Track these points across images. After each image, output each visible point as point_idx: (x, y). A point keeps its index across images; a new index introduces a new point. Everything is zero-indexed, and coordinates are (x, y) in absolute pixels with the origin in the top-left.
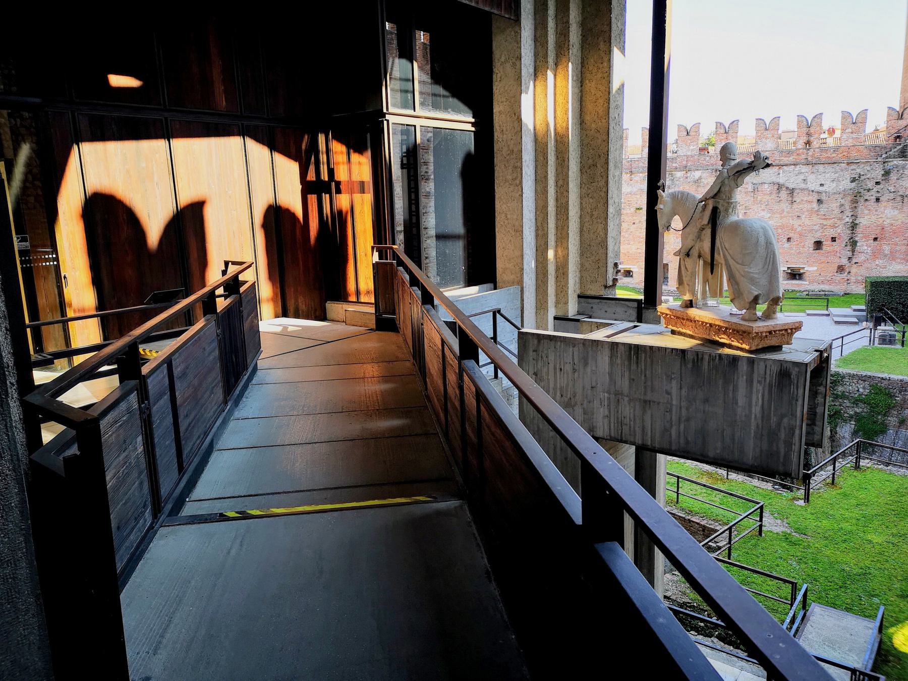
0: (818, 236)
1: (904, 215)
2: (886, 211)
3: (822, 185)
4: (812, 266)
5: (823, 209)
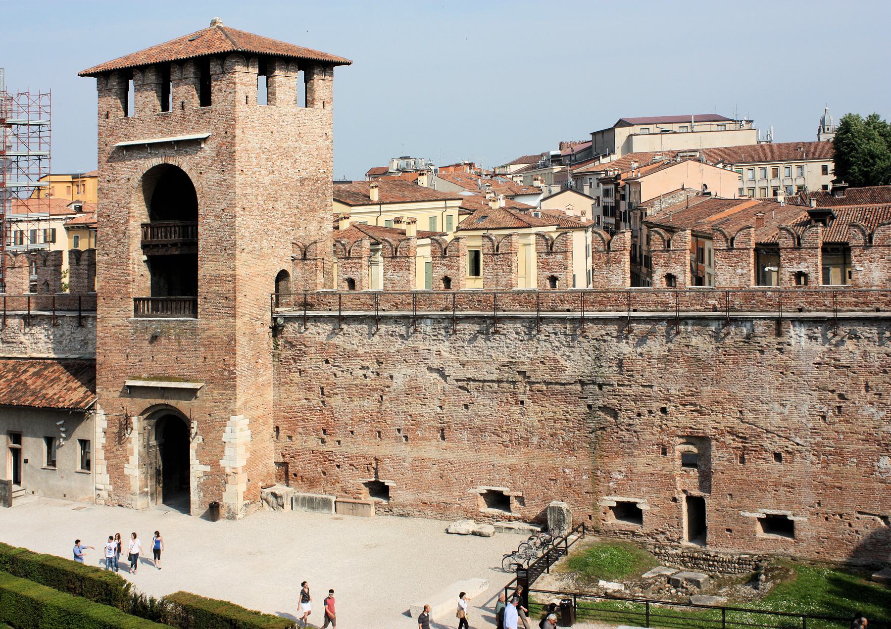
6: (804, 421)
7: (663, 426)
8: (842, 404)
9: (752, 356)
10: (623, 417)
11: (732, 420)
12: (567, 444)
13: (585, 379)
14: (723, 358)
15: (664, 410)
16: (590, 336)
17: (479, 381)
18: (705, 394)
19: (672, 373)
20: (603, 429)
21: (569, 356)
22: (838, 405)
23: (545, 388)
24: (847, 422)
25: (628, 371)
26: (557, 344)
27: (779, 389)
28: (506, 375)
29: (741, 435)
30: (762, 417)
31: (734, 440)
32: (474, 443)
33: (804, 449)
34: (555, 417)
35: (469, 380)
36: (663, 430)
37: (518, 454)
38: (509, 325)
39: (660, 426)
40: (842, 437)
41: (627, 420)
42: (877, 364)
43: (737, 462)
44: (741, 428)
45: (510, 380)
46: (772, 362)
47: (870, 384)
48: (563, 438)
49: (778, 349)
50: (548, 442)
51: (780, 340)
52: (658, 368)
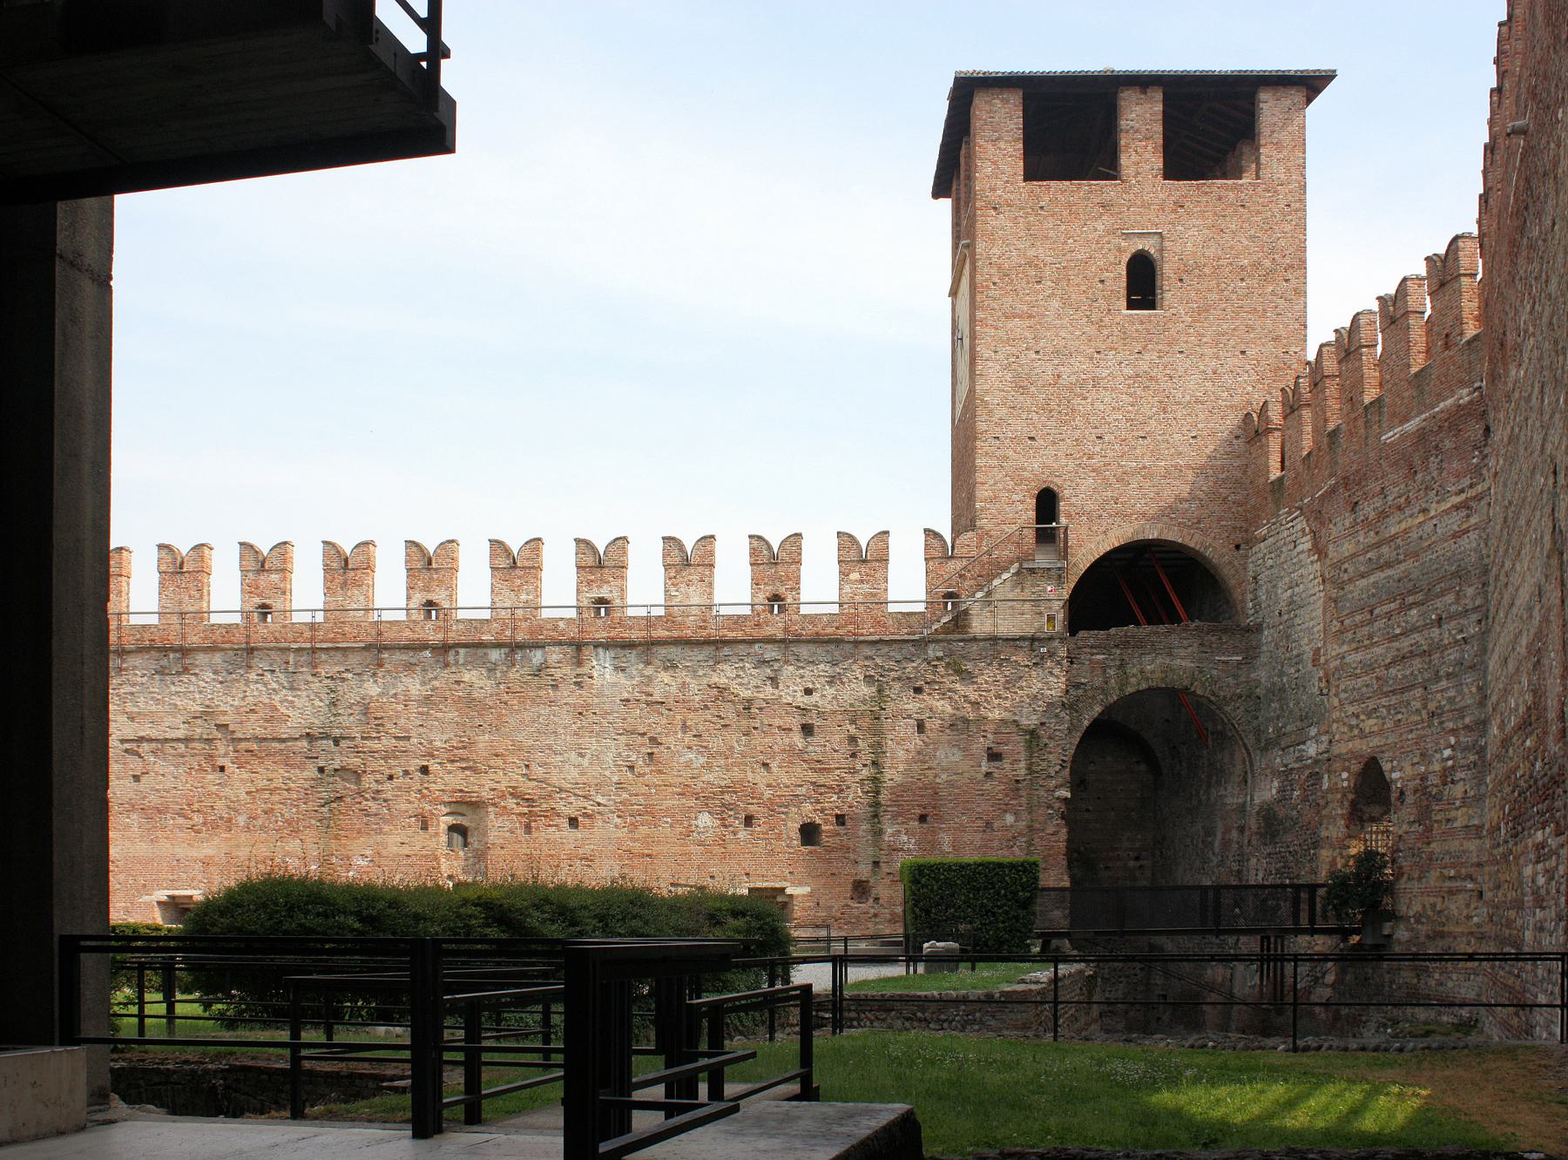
0: (808, 811)
1: (971, 763)
2: (938, 754)
3: (808, 692)
4: (800, 884)
5: (815, 747)
6: (607, 773)
7: (425, 791)
8: (655, 750)
9: (542, 693)
10: (368, 782)
11: (515, 777)
12: (289, 822)
13: (316, 732)
14: (505, 697)
15: (425, 770)
16: (323, 674)
17: (157, 740)
18: (480, 745)
19: (437, 719)
20: (340, 799)
21: (292, 702)
22: (649, 751)
23: (255, 747)
24: (660, 772)
25: (375, 718)
26: (275, 686)
27: (577, 735)
28: (199, 731)
29: (526, 797)
30: (555, 771)
31: (518, 804)
32: (149, 830)
33: (606, 809)
34: (272, 787)
35: (141, 739)
36: (424, 796)
37: (216, 840)
38: (201, 658)
39: (420, 790)
40: (653, 791)
41: (374, 786)
42: (697, 698)
43: (520, 831)
44: (528, 787)
45: (205, 737)
46: (570, 700)
47: (688, 723)
48: (282, 815)
49: (575, 683)
50: (260, 822)
51: (579, 671)
52: (419, 713)
